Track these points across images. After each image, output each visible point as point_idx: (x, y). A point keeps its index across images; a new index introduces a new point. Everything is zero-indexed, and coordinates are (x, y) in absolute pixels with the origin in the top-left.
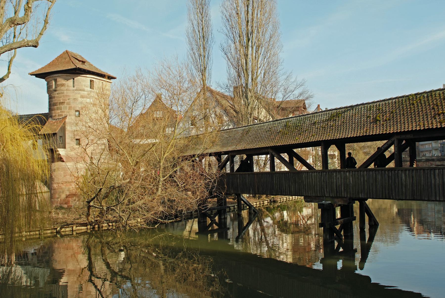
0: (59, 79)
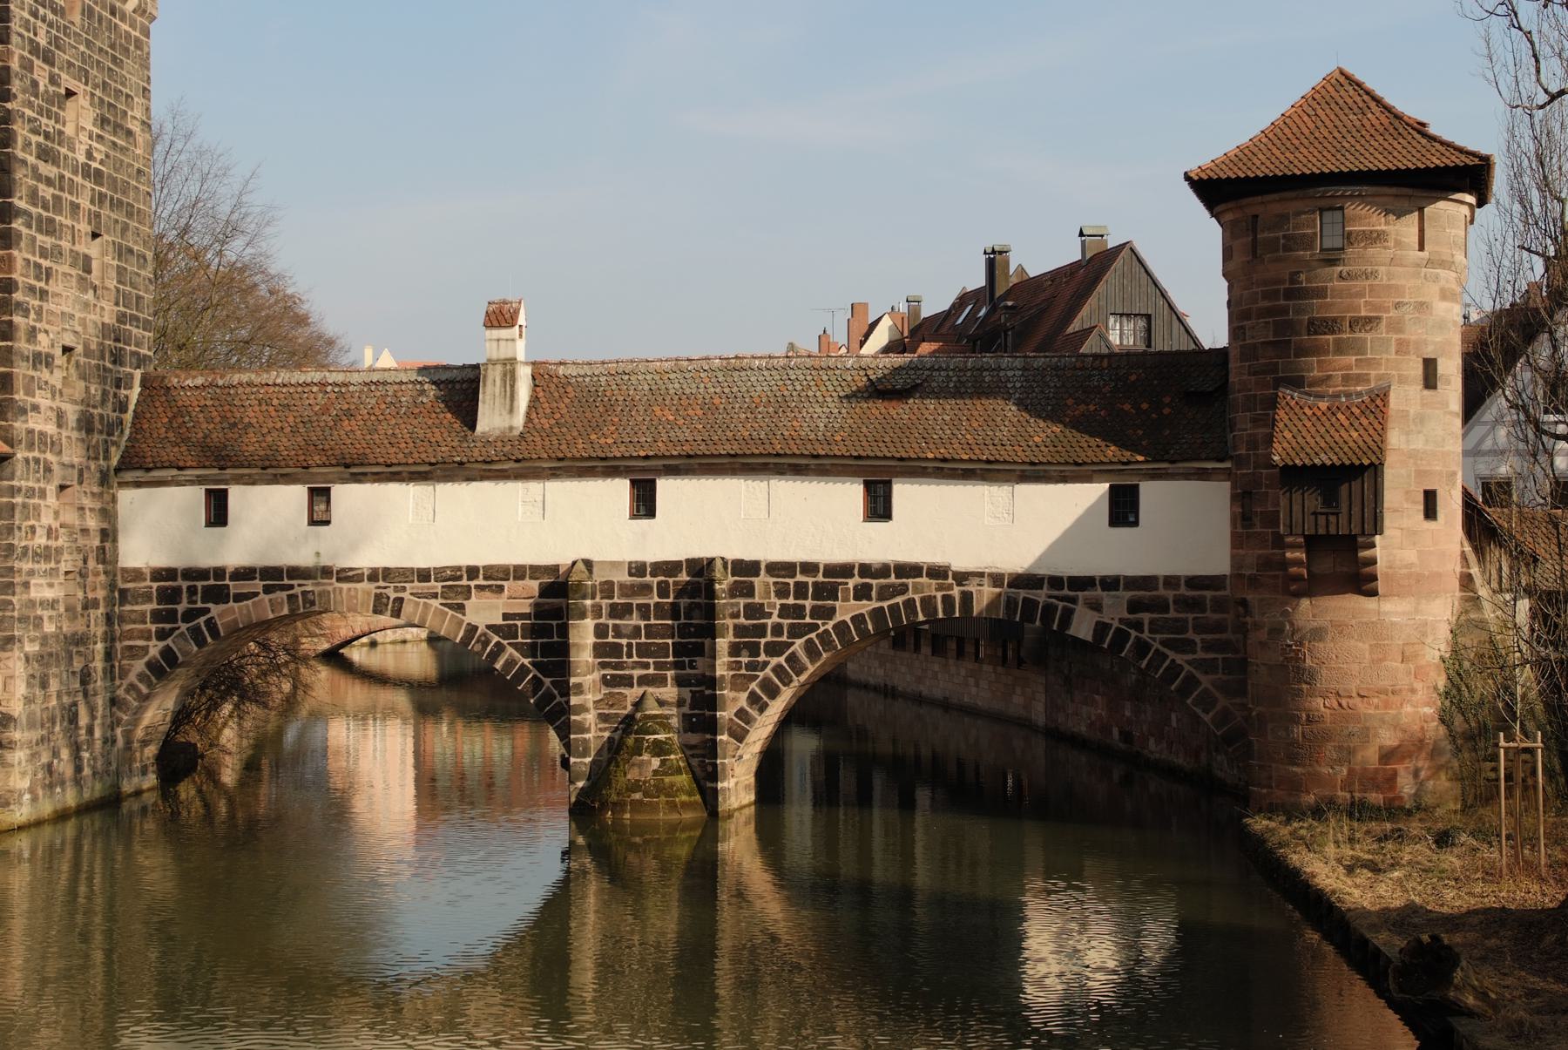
0: (1352, 209)
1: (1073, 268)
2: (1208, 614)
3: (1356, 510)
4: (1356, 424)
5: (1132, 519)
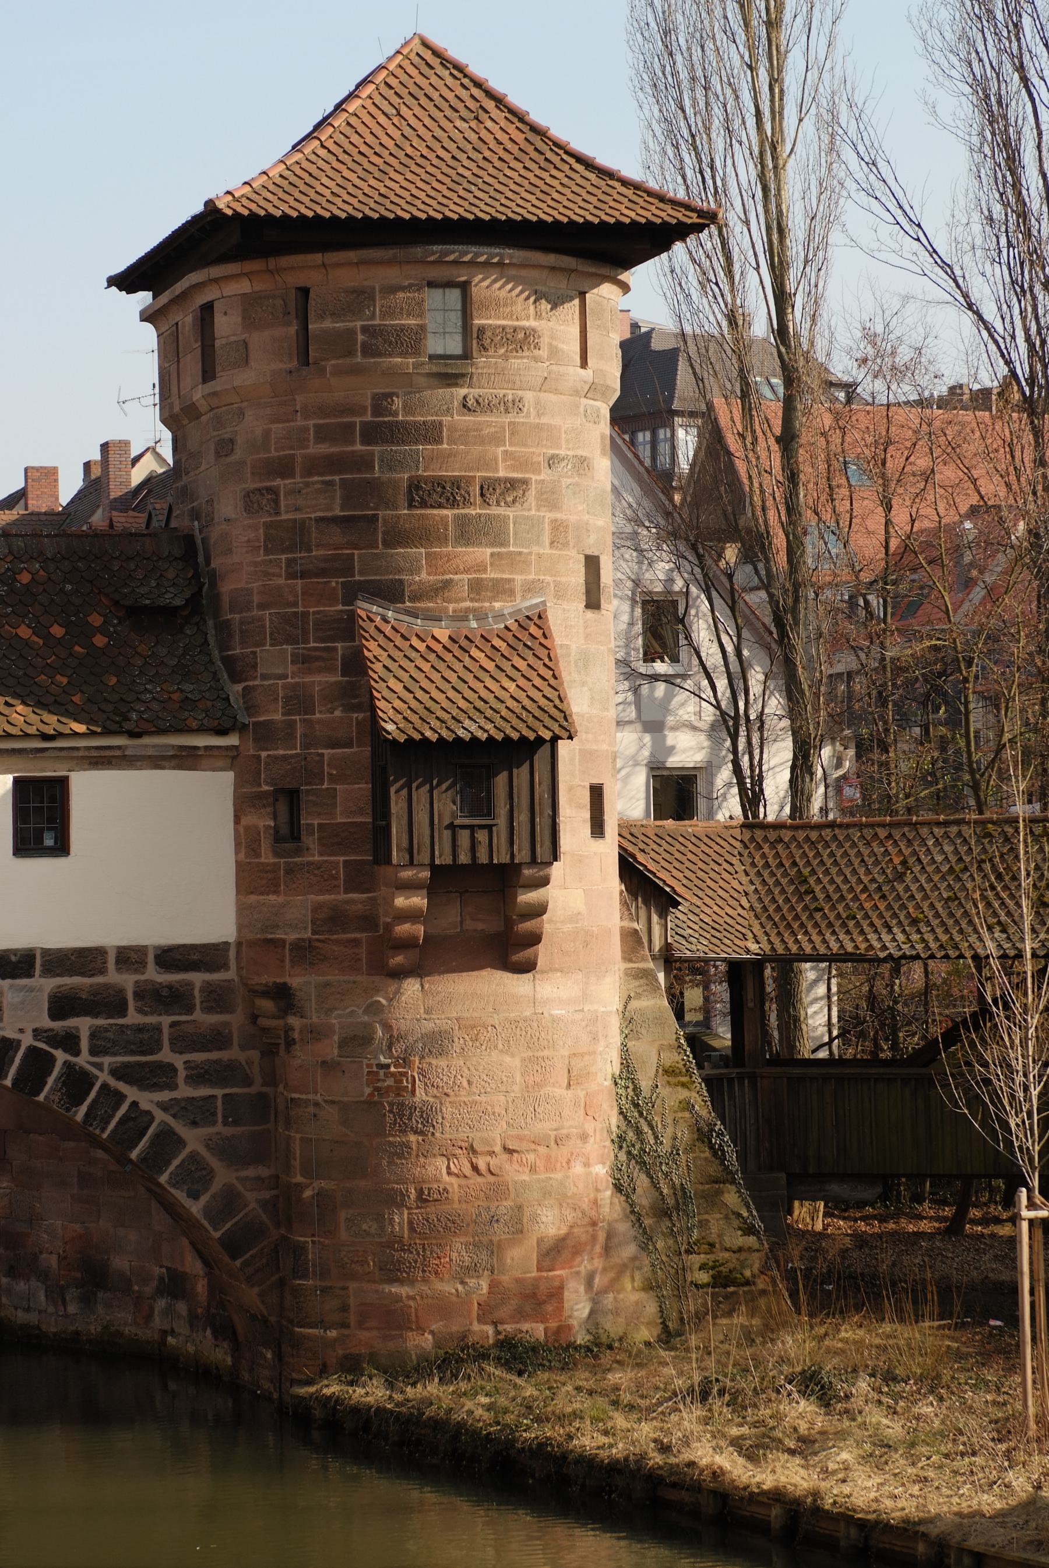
2: (198, 1015)
3: (522, 817)
5: (49, 842)
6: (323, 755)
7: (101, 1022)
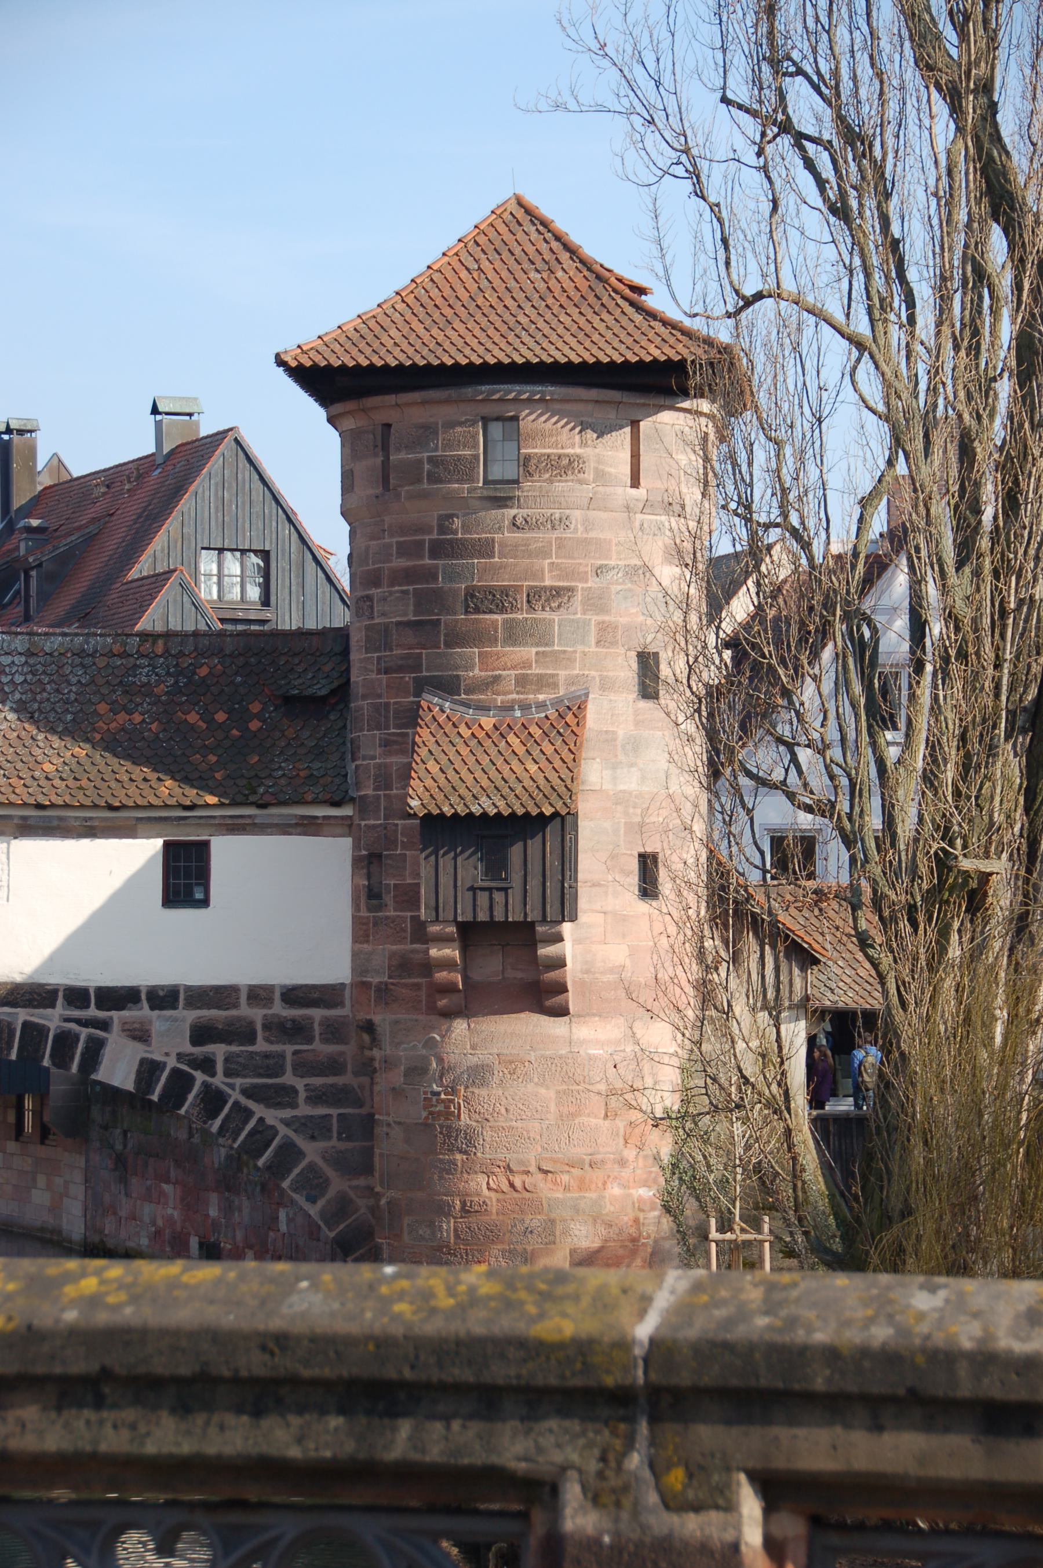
0: (532, 421)
1: (142, 467)
2: (317, 1045)
3: (534, 884)
4: (536, 753)
5: (199, 895)
6: (397, 825)
7: (234, 1048)
